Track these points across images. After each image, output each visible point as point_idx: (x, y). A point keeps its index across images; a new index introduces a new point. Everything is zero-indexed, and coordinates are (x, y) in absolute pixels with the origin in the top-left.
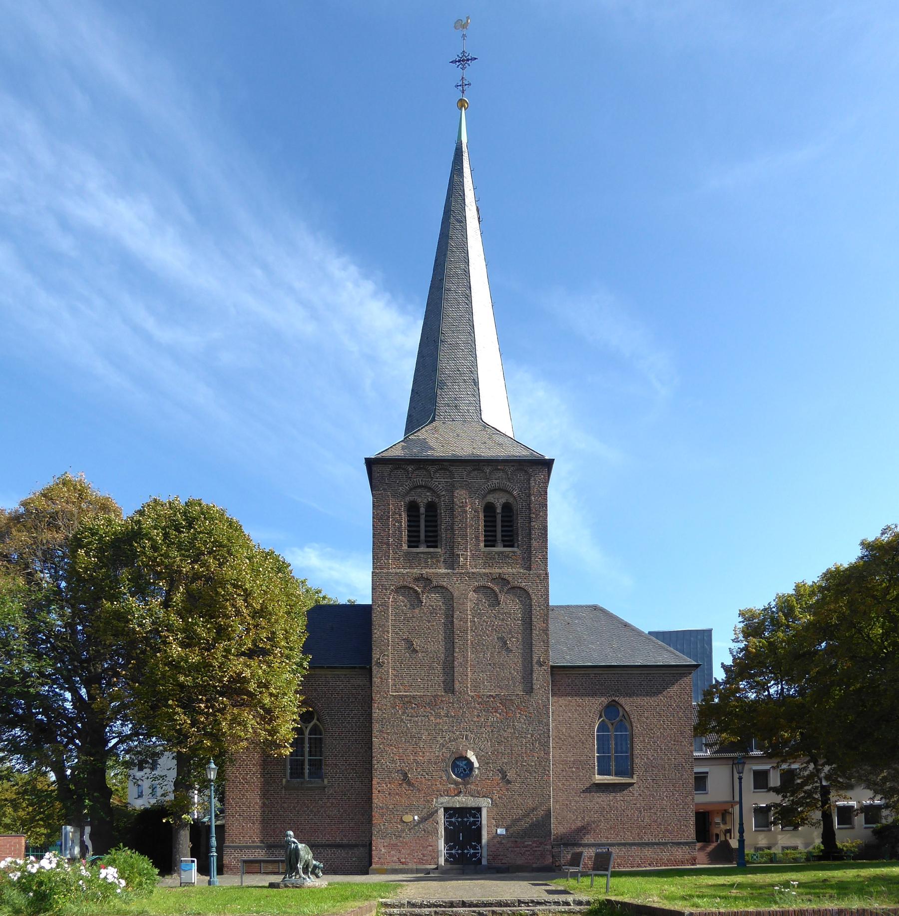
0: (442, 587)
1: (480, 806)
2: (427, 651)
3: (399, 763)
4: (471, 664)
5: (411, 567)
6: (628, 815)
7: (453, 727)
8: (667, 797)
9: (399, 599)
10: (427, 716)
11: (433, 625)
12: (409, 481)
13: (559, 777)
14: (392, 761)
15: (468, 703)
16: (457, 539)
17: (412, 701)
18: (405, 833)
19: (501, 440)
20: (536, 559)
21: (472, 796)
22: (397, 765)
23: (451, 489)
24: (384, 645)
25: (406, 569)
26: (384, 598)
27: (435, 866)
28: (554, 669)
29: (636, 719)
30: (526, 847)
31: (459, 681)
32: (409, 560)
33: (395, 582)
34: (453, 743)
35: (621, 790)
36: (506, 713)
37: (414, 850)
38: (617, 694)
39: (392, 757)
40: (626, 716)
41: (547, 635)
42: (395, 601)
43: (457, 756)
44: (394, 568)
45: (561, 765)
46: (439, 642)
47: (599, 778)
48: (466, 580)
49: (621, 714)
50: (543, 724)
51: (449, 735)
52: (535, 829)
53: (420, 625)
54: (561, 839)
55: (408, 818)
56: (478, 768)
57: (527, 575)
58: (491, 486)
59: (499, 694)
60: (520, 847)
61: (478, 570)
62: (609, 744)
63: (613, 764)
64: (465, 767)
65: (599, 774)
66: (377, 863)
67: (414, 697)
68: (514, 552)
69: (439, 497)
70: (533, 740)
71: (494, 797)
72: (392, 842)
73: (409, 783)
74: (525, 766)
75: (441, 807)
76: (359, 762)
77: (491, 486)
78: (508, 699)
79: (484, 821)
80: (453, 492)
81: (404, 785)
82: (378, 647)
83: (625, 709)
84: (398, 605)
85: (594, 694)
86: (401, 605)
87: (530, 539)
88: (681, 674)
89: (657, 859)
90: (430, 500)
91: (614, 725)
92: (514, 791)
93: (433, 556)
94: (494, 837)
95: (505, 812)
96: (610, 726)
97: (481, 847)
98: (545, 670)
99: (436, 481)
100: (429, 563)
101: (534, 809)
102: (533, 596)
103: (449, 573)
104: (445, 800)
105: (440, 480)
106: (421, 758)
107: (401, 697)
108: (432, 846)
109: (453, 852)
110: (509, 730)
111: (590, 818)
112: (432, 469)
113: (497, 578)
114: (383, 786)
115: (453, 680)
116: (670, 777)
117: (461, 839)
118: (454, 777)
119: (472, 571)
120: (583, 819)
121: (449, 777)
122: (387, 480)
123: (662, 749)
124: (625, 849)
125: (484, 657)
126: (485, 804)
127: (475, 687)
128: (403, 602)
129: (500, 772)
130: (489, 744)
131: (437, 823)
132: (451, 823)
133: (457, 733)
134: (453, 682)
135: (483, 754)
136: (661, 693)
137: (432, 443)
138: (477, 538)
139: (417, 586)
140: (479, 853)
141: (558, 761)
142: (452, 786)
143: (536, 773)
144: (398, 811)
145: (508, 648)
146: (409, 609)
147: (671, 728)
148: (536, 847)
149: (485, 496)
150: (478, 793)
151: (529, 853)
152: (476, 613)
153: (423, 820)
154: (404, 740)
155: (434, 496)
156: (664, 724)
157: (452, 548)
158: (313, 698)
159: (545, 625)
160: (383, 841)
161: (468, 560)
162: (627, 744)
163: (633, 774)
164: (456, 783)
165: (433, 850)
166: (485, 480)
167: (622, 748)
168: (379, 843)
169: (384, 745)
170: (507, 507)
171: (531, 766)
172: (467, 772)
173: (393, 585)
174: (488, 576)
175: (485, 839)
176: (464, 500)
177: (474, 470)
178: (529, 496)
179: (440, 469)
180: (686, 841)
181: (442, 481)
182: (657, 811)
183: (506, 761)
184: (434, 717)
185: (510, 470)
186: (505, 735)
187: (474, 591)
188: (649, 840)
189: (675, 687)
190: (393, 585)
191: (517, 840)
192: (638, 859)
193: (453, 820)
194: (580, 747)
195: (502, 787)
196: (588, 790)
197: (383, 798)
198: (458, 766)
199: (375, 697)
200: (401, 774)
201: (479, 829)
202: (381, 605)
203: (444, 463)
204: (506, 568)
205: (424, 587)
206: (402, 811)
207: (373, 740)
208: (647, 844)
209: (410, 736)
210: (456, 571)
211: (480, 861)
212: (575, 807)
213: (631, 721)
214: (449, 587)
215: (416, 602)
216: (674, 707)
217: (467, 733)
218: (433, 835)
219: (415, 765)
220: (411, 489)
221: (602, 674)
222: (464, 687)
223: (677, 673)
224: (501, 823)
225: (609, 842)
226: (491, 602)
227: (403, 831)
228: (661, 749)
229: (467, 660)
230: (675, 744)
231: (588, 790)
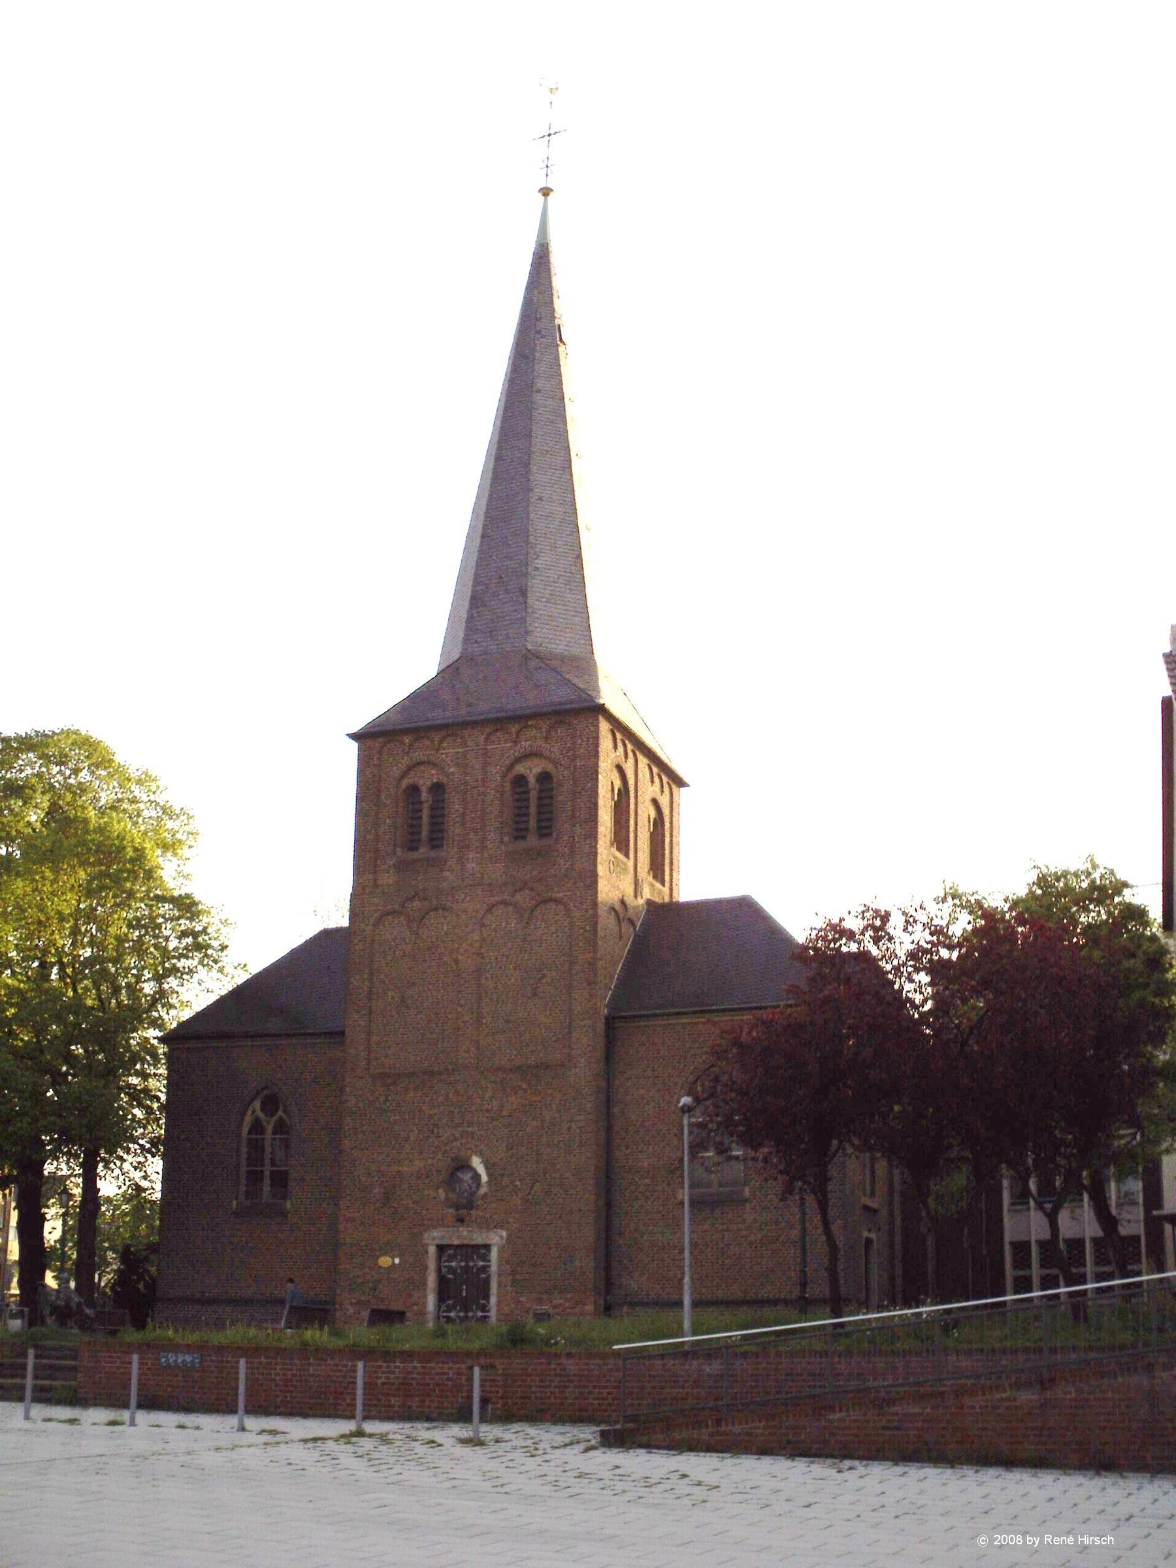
1: (488, 1243)
79: (494, 1268)
117: (464, 1294)
170: (545, 777)
193: (453, 1264)
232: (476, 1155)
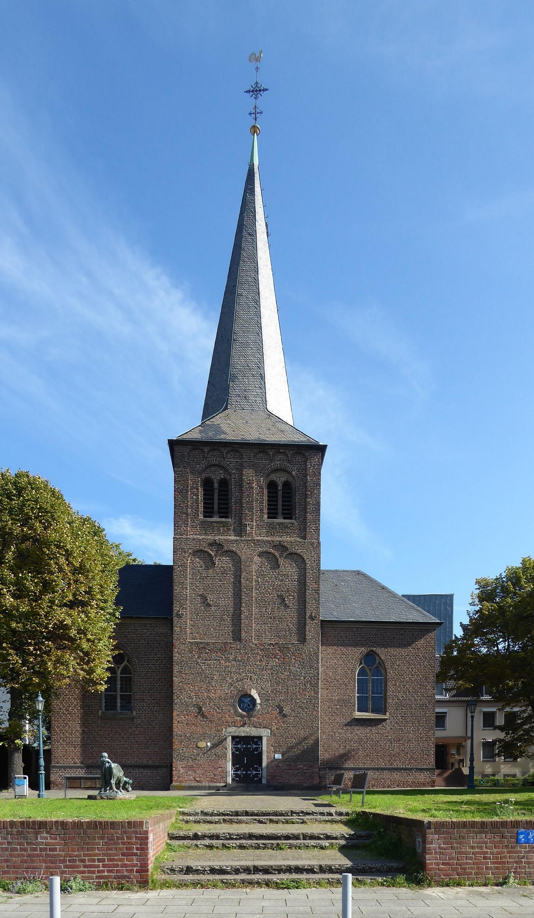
0: (232, 552)
2: (219, 605)
3: (195, 699)
4: (255, 617)
5: (206, 534)
6: (381, 745)
7: (240, 669)
8: (413, 731)
9: (196, 561)
10: (219, 660)
11: (224, 584)
12: (205, 460)
13: (325, 712)
14: (190, 697)
15: (252, 650)
16: (245, 511)
17: (206, 647)
18: (199, 757)
19: (283, 427)
20: (311, 529)
21: (255, 727)
22: (193, 700)
23: (240, 469)
24: (183, 600)
25: (202, 535)
26: (183, 560)
27: (224, 784)
28: (324, 623)
29: (389, 667)
30: (299, 770)
31: (245, 631)
32: (204, 528)
33: (193, 546)
34: (240, 683)
35: (375, 725)
36: (284, 658)
37: (207, 771)
38: (375, 646)
39: (189, 694)
40: (382, 664)
41: (318, 594)
42: (192, 562)
43: (243, 694)
44: (192, 534)
45: (328, 703)
46: (229, 598)
47: (358, 715)
48: (252, 546)
49: (377, 662)
50: (313, 669)
51: (236, 676)
52: (305, 755)
53: (213, 583)
54: (327, 764)
55: (202, 744)
56: (260, 704)
57: (303, 543)
58: (274, 467)
59: (278, 643)
60: (292, 770)
61: (262, 538)
62: (367, 687)
63: (370, 703)
64: (249, 703)
65: (358, 711)
66: (176, 781)
67: (208, 644)
68: (292, 524)
69: (230, 474)
70: (305, 682)
71: (273, 728)
72: (189, 764)
73: (203, 716)
74: (298, 703)
75: (229, 736)
76: (162, 698)
77: (274, 467)
78: (285, 648)
79: (265, 748)
80: (242, 471)
81: (199, 717)
82: (178, 601)
83: (381, 658)
84: (195, 566)
85: (356, 644)
86: (197, 566)
87: (306, 513)
88: (427, 630)
89: (404, 782)
90: (222, 477)
91: (372, 670)
92: (289, 723)
93: (225, 525)
94: (272, 761)
95: (281, 741)
96: (368, 671)
97: (261, 769)
98: (316, 624)
99: (228, 461)
100: (221, 531)
101: (305, 739)
102: (307, 561)
103: (237, 540)
104: (233, 730)
105: (231, 460)
106: (213, 695)
107: (197, 643)
108: (221, 768)
109: (239, 772)
110: (286, 673)
111: (350, 747)
112: (225, 450)
113: (277, 545)
114: (182, 718)
115: (241, 630)
116: (416, 715)
118: (240, 711)
119: (257, 538)
120: (345, 747)
121: (236, 711)
122: (186, 459)
123: (410, 691)
124: (378, 772)
125: (266, 612)
126: (265, 733)
127: (258, 637)
128: (199, 563)
129: (278, 708)
130: (269, 684)
131: (226, 749)
132: (237, 749)
133: (243, 674)
134: (240, 631)
135: (264, 692)
136: (411, 645)
137: (225, 428)
138: (261, 510)
139: (211, 550)
140: (259, 774)
141: (325, 700)
142: (239, 718)
143: (307, 709)
144: (194, 738)
145: (286, 604)
146: (204, 569)
147: (418, 674)
148: (306, 770)
149: (268, 475)
150: (260, 724)
151: (300, 774)
152: (260, 574)
153: (214, 746)
154: (199, 680)
155: (226, 474)
156: (412, 671)
157: (241, 519)
158: (124, 643)
159: (317, 586)
160: (181, 763)
161: (254, 529)
162: (381, 687)
163: (386, 711)
164: (242, 716)
165: (222, 771)
166: (268, 462)
167: (377, 690)
168: (178, 765)
169: (182, 683)
170: (287, 485)
171: (304, 703)
172: (251, 707)
173: (191, 549)
174: (270, 543)
175: (264, 764)
176: (251, 478)
177: (260, 452)
178: (306, 476)
179: (231, 451)
180: (427, 767)
181: (233, 461)
182: (405, 742)
183: (283, 698)
184: (224, 661)
185: (290, 453)
186: (283, 677)
187: (258, 556)
188: (397, 766)
189: (422, 641)
190: (191, 549)
191: (291, 763)
192: (388, 781)
194: (343, 688)
195: (279, 720)
196: (349, 724)
197: (182, 727)
198: (244, 702)
199: (176, 643)
200: (197, 708)
201: (261, 754)
202: (181, 566)
203: (234, 446)
204: (285, 537)
205: (217, 552)
206: (197, 739)
207: (174, 679)
208: (397, 769)
209: (204, 677)
210: (243, 539)
211: (261, 780)
212: (338, 738)
213: (385, 668)
214: (238, 552)
215: (210, 563)
216: (421, 658)
217: (251, 675)
218: (223, 758)
219: (208, 700)
220: (207, 467)
221: (362, 628)
222: (249, 636)
223: (424, 629)
224: (278, 750)
225: (366, 766)
226: (272, 565)
227: (198, 755)
228: (409, 692)
229: (252, 614)
230: (420, 688)
231: (349, 724)
232: (253, 689)
